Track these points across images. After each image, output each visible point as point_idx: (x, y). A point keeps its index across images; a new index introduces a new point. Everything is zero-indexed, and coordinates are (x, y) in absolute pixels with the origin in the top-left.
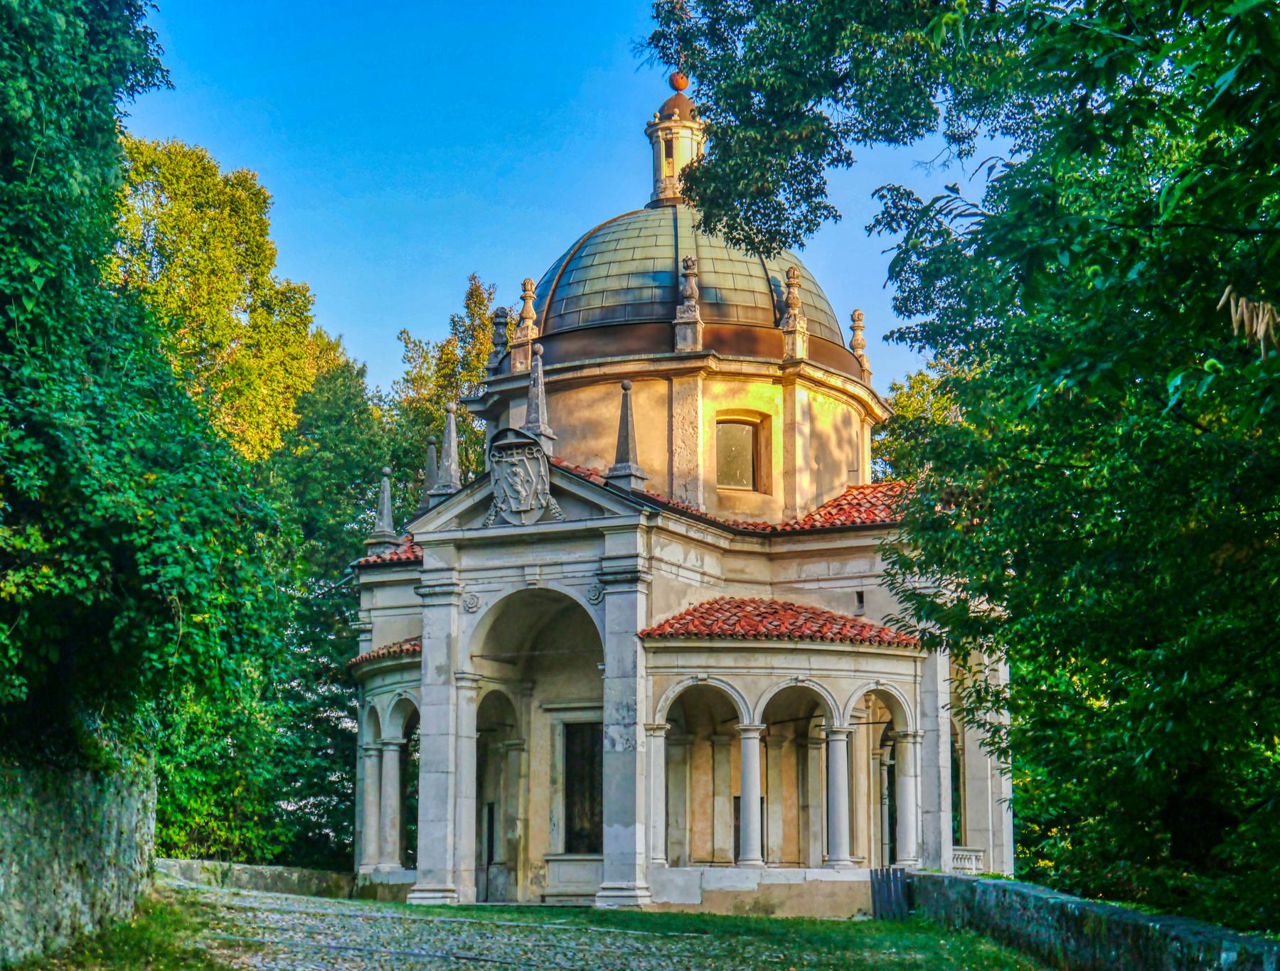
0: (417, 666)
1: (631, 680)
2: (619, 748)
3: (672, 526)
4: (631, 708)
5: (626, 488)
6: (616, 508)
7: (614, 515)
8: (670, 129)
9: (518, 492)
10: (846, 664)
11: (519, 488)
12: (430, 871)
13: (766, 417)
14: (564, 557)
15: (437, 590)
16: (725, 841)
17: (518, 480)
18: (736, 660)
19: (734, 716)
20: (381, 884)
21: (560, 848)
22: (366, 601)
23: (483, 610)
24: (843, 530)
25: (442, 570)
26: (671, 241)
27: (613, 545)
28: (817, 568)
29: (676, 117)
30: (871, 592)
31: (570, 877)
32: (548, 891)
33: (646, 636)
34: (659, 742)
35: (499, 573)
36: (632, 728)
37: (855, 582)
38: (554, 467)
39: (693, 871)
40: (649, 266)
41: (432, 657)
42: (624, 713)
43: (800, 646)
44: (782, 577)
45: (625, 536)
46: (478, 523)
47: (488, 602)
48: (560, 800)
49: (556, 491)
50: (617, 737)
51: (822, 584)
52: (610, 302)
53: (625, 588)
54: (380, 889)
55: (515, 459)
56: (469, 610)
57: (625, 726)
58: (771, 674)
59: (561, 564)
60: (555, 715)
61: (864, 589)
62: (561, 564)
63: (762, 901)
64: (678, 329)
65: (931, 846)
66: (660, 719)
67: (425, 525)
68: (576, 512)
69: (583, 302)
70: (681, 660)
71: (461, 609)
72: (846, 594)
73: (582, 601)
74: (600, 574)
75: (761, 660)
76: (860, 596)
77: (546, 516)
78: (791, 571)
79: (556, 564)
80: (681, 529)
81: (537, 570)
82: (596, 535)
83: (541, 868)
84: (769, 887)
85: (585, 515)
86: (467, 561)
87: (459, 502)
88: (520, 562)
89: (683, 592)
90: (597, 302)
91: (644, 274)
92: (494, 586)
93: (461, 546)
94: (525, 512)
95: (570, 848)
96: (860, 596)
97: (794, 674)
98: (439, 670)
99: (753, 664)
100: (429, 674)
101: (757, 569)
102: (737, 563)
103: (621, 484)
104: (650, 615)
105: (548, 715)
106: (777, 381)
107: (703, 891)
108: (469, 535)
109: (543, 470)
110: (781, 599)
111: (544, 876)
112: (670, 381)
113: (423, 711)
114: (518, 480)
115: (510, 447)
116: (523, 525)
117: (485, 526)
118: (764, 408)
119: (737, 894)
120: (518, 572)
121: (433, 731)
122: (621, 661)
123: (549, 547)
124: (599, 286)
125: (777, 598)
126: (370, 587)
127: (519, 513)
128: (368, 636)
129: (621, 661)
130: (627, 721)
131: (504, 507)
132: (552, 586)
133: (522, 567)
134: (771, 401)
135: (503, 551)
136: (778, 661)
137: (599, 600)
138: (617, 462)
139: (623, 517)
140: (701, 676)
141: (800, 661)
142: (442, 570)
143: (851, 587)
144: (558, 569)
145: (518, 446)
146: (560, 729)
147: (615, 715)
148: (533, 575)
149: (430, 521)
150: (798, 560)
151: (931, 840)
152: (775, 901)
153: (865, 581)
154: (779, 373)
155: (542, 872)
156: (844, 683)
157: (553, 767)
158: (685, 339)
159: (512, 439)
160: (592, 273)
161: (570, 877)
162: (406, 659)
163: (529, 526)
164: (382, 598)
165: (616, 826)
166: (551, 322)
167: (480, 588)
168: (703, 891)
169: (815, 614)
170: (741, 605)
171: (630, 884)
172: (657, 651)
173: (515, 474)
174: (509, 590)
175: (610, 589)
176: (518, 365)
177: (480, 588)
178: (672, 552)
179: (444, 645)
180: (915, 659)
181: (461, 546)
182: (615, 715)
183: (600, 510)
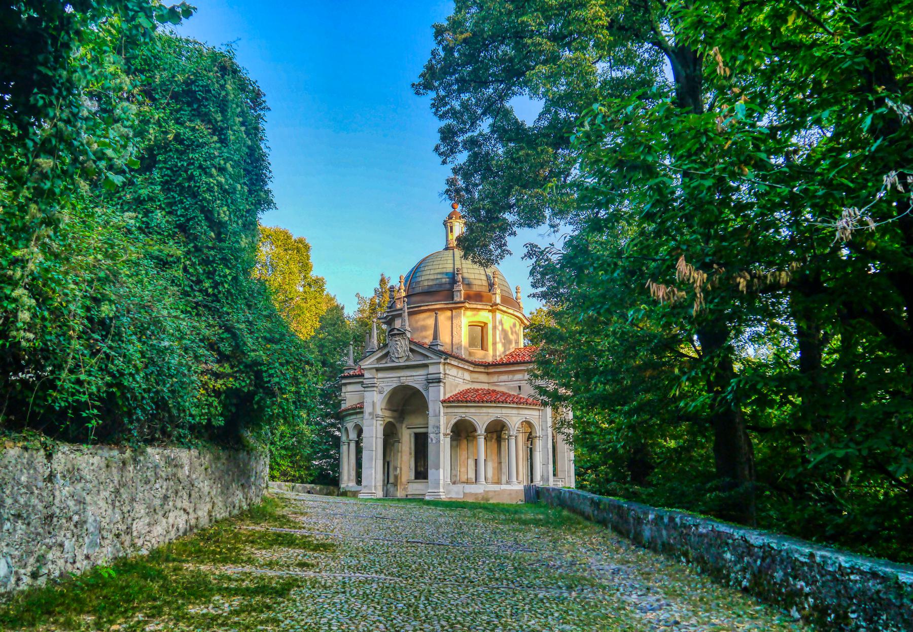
0: (362, 412)
3: (453, 362)
4: (438, 427)
6: (432, 356)
10: (515, 411)
13: (486, 324)
14: (415, 374)
16: (472, 475)
19: (475, 430)
21: (413, 478)
22: (344, 389)
24: (513, 364)
27: (432, 369)
28: (504, 377)
31: (417, 488)
33: (444, 402)
34: (448, 439)
38: (411, 342)
39: (460, 486)
40: (444, 270)
41: (368, 409)
46: (384, 362)
47: (387, 390)
49: (412, 350)
52: (430, 283)
56: (380, 393)
65: (545, 477)
66: (449, 431)
68: (419, 357)
70: (456, 410)
74: (427, 379)
75: (485, 410)
76: (520, 387)
77: (408, 359)
78: (495, 379)
80: (456, 364)
82: (426, 366)
86: (380, 375)
89: (457, 386)
90: (426, 283)
95: (416, 478)
96: (520, 387)
98: (370, 414)
100: (366, 415)
101: (483, 378)
102: (476, 376)
103: (435, 347)
104: (445, 394)
106: (490, 311)
107: (464, 494)
109: (407, 343)
110: (492, 388)
113: (364, 428)
115: (395, 334)
118: (485, 321)
119: (476, 494)
122: (435, 411)
124: (427, 277)
126: (345, 384)
129: (435, 411)
132: (410, 384)
137: (427, 389)
139: (435, 359)
141: (498, 411)
143: (517, 384)
145: (398, 334)
146: (413, 435)
148: (403, 380)
151: (545, 474)
159: (396, 332)
160: (424, 273)
161: (417, 488)
162: (358, 410)
163: (402, 363)
164: (350, 388)
168: (464, 494)
169: (504, 394)
170: (477, 390)
172: (447, 407)
174: (395, 385)
178: (453, 372)
183: (427, 357)
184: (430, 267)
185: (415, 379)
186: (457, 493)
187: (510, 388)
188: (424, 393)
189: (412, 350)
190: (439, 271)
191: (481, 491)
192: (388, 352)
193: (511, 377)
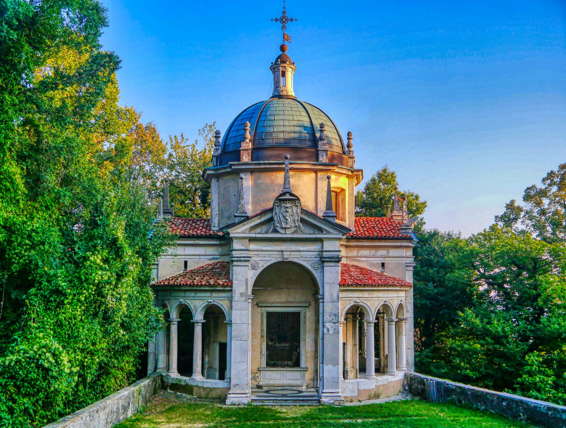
1: (336, 304)
2: (331, 332)
4: (336, 315)
5: (333, 221)
7: (328, 233)
8: (285, 67)
9: (287, 220)
11: (288, 218)
12: (237, 385)
13: (343, 190)
14: (301, 249)
15: (242, 259)
17: (288, 214)
18: (368, 294)
20: (197, 386)
25: (244, 250)
26: (306, 114)
27: (328, 246)
29: (287, 63)
30: (388, 263)
32: (261, 383)
35: (269, 253)
36: (337, 324)
37: (381, 259)
40: (301, 123)
42: (333, 317)
43: (389, 289)
44: (349, 255)
45: (333, 242)
46: (259, 230)
49: (302, 220)
50: (330, 328)
51: (368, 259)
52: (288, 136)
53: (333, 264)
54: (195, 389)
55: (288, 205)
56: (254, 268)
58: (378, 300)
59: (300, 251)
60: (263, 309)
61: (385, 262)
62: (300, 251)
63: (376, 392)
64: (319, 152)
67: (236, 229)
69: (274, 135)
70: (350, 294)
71: (250, 267)
72: (378, 263)
73: (310, 268)
75: (376, 294)
76: (383, 265)
78: (354, 253)
81: (289, 253)
83: (256, 373)
84: (379, 386)
85: (312, 231)
86: (253, 246)
87: (254, 221)
88: (279, 249)
90: (281, 136)
91: (300, 126)
92: (268, 259)
93: (251, 240)
94: (288, 228)
95: (268, 365)
96: (383, 265)
97: (385, 299)
98: (242, 295)
99: (373, 296)
103: (331, 219)
105: (260, 308)
106: (348, 176)
108: (254, 235)
110: (351, 263)
111: (258, 377)
112: (316, 173)
114: (288, 214)
115: (286, 200)
116: (286, 234)
117: (267, 232)
118: (344, 187)
119: (369, 391)
120: (280, 253)
121: (239, 322)
122: (331, 295)
123: (294, 243)
124: (281, 129)
125: (348, 263)
127: (285, 228)
128: (156, 266)
129: (331, 295)
130: (334, 321)
131: (278, 225)
132: (295, 260)
133: (282, 251)
134: (345, 184)
135: (271, 243)
136: (380, 294)
138: (327, 209)
140: (358, 301)
141: (385, 294)
142: (241, 250)
144: (299, 253)
145: (289, 200)
146: (265, 315)
147: (329, 318)
149: (239, 228)
150: (358, 249)
152: (380, 392)
153: (386, 259)
154: (351, 174)
155: (257, 375)
156: (395, 301)
157: (262, 330)
158: (323, 156)
159: (288, 197)
160: (276, 123)
165: (330, 365)
166: (257, 141)
167: (260, 259)
171: (337, 390)
173: (287, 212)
174: (274, 261)
175: (326, 264)
176: (244, 158)
177: (260, 259)
179: (244, 284)
180: (406, 291)
181: (251, 240)
182: (329, 318)
183: (320, 230)
184: (282, 117)
185: (304, 255)
186: (352, 391)
187: (372, 265)
188: (316, 274)
190: (294, 123)
191: (373, 386)
192: (271, 220)
193: (373, 252)
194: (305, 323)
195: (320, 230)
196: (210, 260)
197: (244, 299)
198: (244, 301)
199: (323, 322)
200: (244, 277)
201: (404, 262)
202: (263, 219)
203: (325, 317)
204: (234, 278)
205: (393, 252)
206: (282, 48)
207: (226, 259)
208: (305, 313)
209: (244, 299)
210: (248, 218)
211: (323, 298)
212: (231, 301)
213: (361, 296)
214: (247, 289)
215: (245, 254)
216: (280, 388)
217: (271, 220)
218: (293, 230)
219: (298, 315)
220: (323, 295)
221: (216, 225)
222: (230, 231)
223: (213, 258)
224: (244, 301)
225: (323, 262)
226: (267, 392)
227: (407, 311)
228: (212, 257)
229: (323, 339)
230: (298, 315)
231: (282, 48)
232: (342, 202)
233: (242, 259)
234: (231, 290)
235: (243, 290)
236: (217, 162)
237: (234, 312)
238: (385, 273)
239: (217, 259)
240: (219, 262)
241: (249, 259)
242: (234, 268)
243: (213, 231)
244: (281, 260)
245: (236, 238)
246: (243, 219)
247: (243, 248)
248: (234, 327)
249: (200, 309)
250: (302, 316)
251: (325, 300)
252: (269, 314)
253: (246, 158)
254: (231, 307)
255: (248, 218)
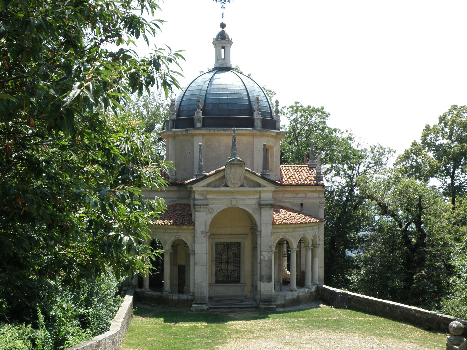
7: (265, 187)
13: (272, 147)
23: (216, 213)
28: (289, 195)
42: (268, 248)
48: (214, 266)
50: (266, 255)
57: (268, 252)
70: (280, 231)
77: (242, 186)
79: (242, 199)
86: (209, 197)
93: (208, 192)
95: (217, 282)
96: (302, 204)
98: (202, 232)
115: (234, 164)
130: (269, 251)
132: (240, 207)
136: (301, 229)
143: (300, 201)
146: (214, 244)
183: (259, 185)
188: (256, 217)
189: (246, 178)
192: (224, 177)
193: (294, 195)
194: (244, 250)
195: (259, 185)
196: (170, 202)
197: (203, 235)
198: (204, 237)
199: (261, 251)
200: (202, 219)
201: (318, 202)
202: (217, 177)
203: (262, 248)
204: (196, 220)
205: (309, 195)
206: (223, 26)
207: (183, 202)
208: (244, 243)
209: (203, 235)
210: (206, 177)
211: (261, 234)
212: (194, 237)
213: (287, 231)
214: (206, 228)
215: (204, 202)
216: (226, 299)
217: (224, 177)
218: (240, 185)
219: (239, 244)
220: (261, 232)
221: (174, 174)
222: (193, 186)
223: (173, 201)
224: (204, 237)
225: (261, 208)
226: (218, 301)
227: (320, 240)
228: (172, 200)
229: (260, 263)
230: (239, 244)
231: (223, 26)
232: (271, 157)
233: (202, 206)
234: (194, 229)
235: (203, 229)
236: (173, 125)
237: (196, 245)
238: (303, 211)
239: (175, 201)
240: (177, 204)
241: (207, 206)
242: (196, 213)
243: (172, 179)
244: (230, 206)
245: (198, 191)
246: (202, 176)
247: (202, 198)
248: (197, 256)
249: (169, 242)
250: (242, 245)
251: (262, 235)
252: (217, 244)
253: (199, 125)
254: (194, 241)
255: (206, 177)
